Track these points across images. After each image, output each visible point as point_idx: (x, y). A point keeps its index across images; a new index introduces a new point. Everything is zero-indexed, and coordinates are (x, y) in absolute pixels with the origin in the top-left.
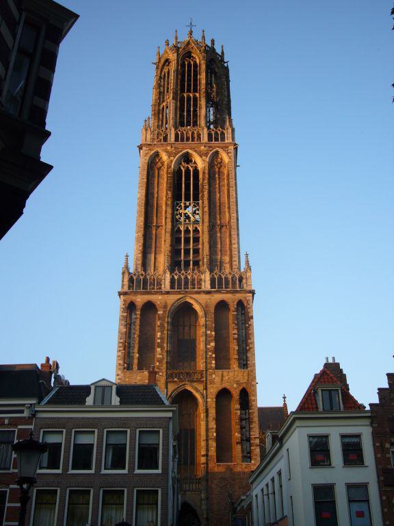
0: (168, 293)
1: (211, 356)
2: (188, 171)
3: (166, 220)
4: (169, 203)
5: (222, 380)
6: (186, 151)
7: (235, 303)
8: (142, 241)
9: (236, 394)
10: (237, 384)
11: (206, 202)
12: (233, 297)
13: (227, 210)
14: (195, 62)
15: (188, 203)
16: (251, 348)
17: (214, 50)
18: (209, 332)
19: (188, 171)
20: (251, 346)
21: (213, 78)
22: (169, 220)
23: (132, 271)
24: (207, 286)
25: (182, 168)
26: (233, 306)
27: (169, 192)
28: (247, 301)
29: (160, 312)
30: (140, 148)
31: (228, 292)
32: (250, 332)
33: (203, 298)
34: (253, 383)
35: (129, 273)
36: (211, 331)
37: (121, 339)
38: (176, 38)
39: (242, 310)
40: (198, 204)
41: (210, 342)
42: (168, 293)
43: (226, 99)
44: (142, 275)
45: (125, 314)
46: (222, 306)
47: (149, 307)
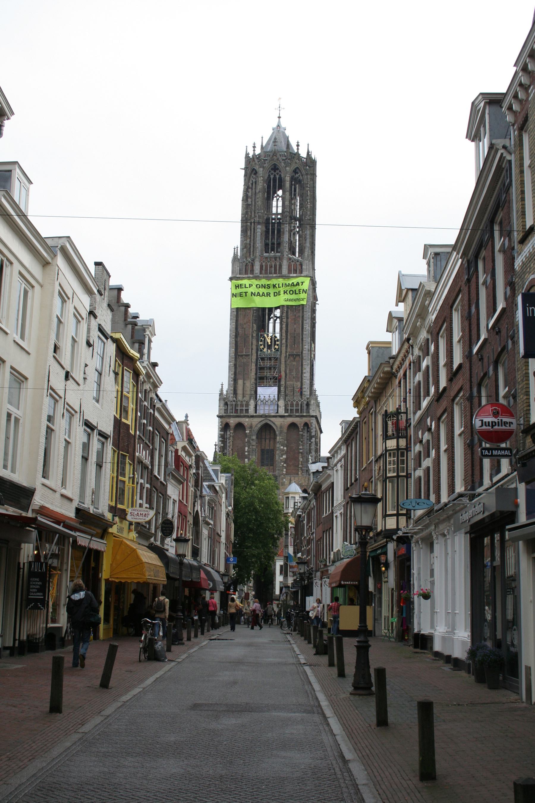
0: (252, 416)
1: (283, 465)
4: (254, 335)
7: (302, 425)
8: (233, 370)
14: (280, 175)
17: (299, 154)
18: (282, 447)
22: (254, 351)
24: (282, 411)
26: (301, 427)
27: (254, 325)
29: (247, 432)
31: (297, 416)
36: (284, 447)
42: (252, 416)
44: (234, 401)
45: (223, 433)
46: (293, 425)
47: (240, 426)
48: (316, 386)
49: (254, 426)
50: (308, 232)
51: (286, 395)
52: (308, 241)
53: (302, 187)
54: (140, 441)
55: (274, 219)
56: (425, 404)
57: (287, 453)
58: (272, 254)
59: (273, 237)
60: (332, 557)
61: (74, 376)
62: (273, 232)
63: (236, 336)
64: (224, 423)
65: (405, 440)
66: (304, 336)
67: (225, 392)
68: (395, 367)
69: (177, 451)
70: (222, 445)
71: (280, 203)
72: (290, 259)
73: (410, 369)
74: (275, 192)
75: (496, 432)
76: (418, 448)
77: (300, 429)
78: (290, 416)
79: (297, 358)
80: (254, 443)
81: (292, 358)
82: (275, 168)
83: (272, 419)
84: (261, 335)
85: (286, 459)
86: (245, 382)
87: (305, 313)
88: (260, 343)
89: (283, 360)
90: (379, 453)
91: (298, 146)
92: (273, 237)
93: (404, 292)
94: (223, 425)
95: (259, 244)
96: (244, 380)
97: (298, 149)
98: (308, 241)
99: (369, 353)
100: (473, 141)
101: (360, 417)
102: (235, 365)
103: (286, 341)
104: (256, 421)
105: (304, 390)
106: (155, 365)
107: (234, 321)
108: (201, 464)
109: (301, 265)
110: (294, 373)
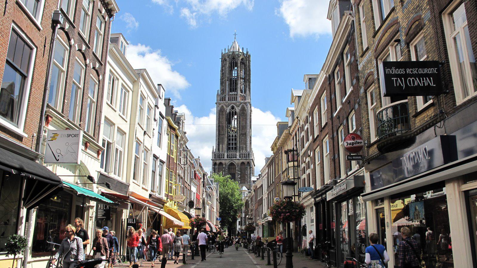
0: (226, 160)
2: (233, 112)
4: (226, 126)
6: (232, 105)
19: (233, 112)
22: (226, 133)
24: (238, 157)
26: (246, 163)
29: (224, 166)
30: (216, 103)
31: (244, 159)
41: (239, 175)
47: (221, 164)
48: (252, 147)
50: (248, 84)
51: (240, 151)
52: (248, 87)
53: (245, 66)
54: (179, 166)
55: (233, 79)
56: (306, 145)
57: (240, 175)
58: (233, 93)
59: (233, 86)
60: (263, 216)
61: (148, 133)
62: (233, 84)
63: (219, 126)
64: (214, 162)
65: (297, 162)
67: (214, 150)
68: (291, 131)
69: (195, 171)
71: (236, 72)
72: (240, 95)
73: (298, 131)
74: (234, 68)
75: (355, 147)
76: (303, 165)
78: (241, 159)
79: (244, 135)
80: (227, 171)
81: (242, 135)
82: (234, 58)
83: (234, 161)
85: (240, 177)
89: (238, 136)
90: (284, 169)
91: (243, 49)
92: (233, 86)
93: (294, 98)
95: (227, 89)
96: (222, 145)
97: (243, 50)
98: (248, 87)
99: (278, 127)
100: (330, 20)
101: (274, 155)
102: (219, 139)
103: (240, 128)
104: (227, 161)
105: (247, 148)
106: (185, 133)
108: (205, 178)
109: (245, 97)
110: (243, 141)
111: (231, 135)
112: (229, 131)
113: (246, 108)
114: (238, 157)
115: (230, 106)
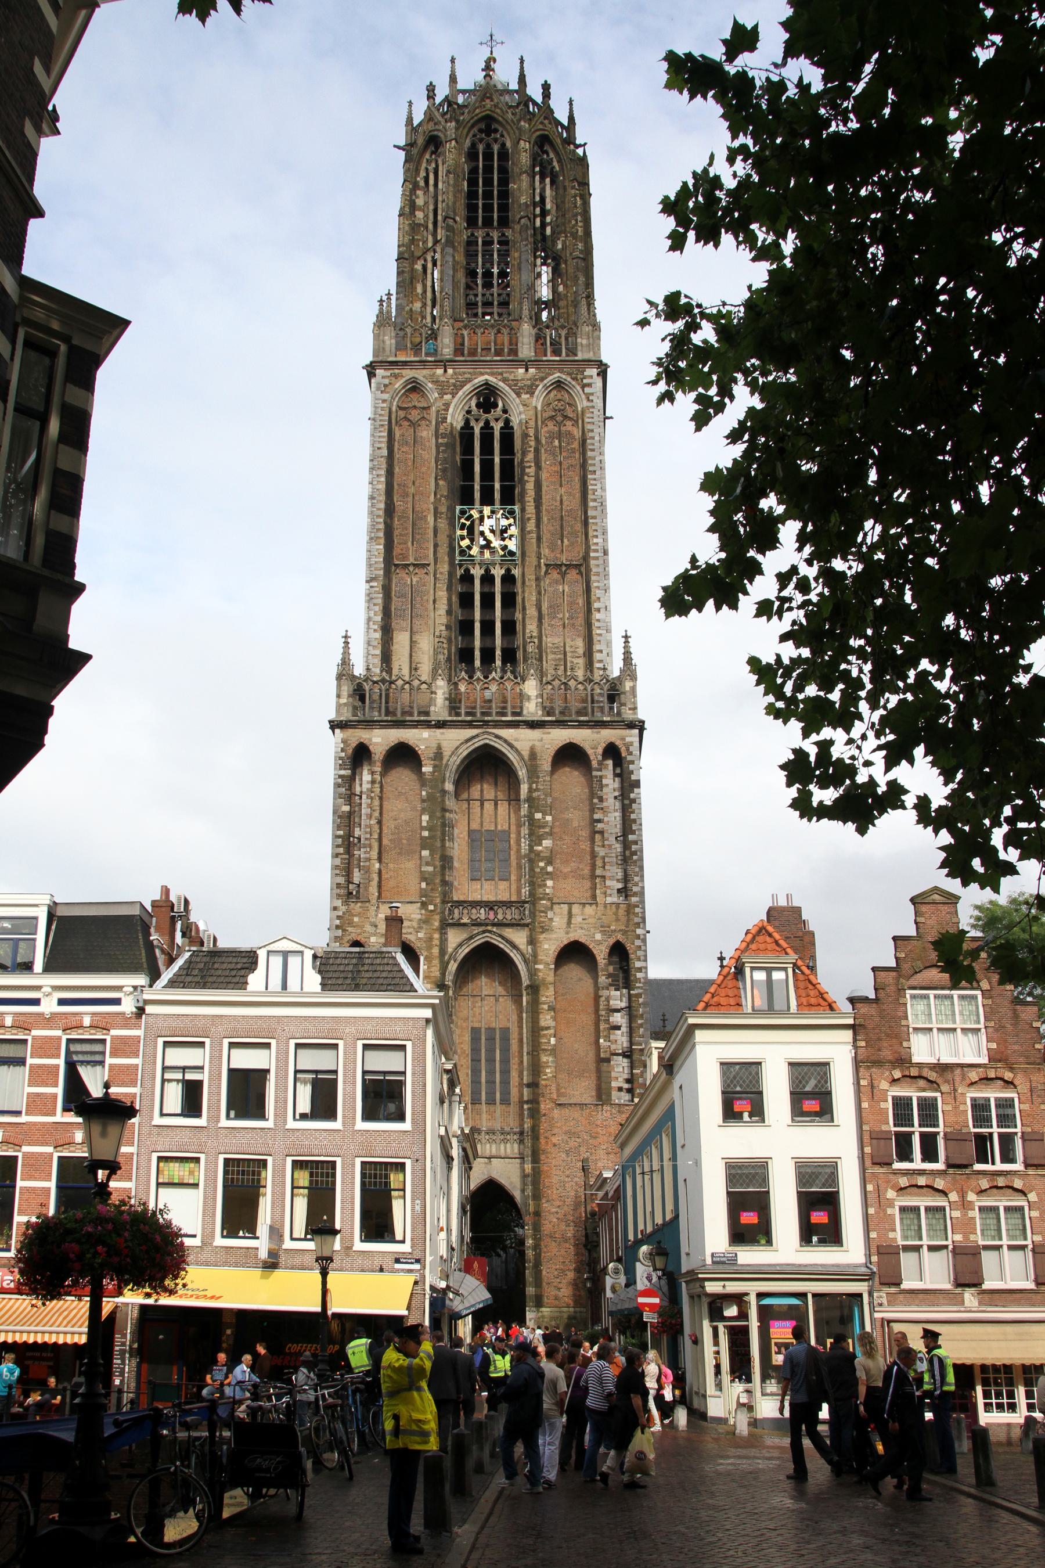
2: (487, 426)
3: (435, 552)
4: (443, 509)
5: (569, 923)
6: (481, 379)
7: (600, 750)
8: (380, 601)
9: (601, 953)
10: (603, 932)
11: (530, 509)
12: (595, 736)
13: (579, 527)
15: (487, 510)
16: (635, 853)
19: (487, 426)
20: (634, 847)
21: (548, 187)
23: (359, 670)
24: (532, 709)
25: (473, 423)
26: (595, 754)
27: (441, 483)
28: (628, 746)
31: (582, 725)
32: (633, 816)
33: (523, 739)
34: (639, 931)
35: (353, 677)
37: (339, 828)
38: (453, 79)
39: (615, 766)
40: (512, 513)
42: (441, 725)
43: (580, 246)
49: (446, 754)
63: (390, 510)
66: (590, 513)
70: (346, 808)
77: (595, 764)
79: (572, 575)
81: (555, 575)
83: (506, 733)
84: (463, 512)
86: (415, 638)
87: (589, 454)
88: (459, 532)
89: (530, 577)
94: (350, 751)
103: (538, 525)
107: (383, 472)
111: (477, 572)
112: (465, 543)
113: (581, 404)
114: (532, 709)
115: (468, 387)
